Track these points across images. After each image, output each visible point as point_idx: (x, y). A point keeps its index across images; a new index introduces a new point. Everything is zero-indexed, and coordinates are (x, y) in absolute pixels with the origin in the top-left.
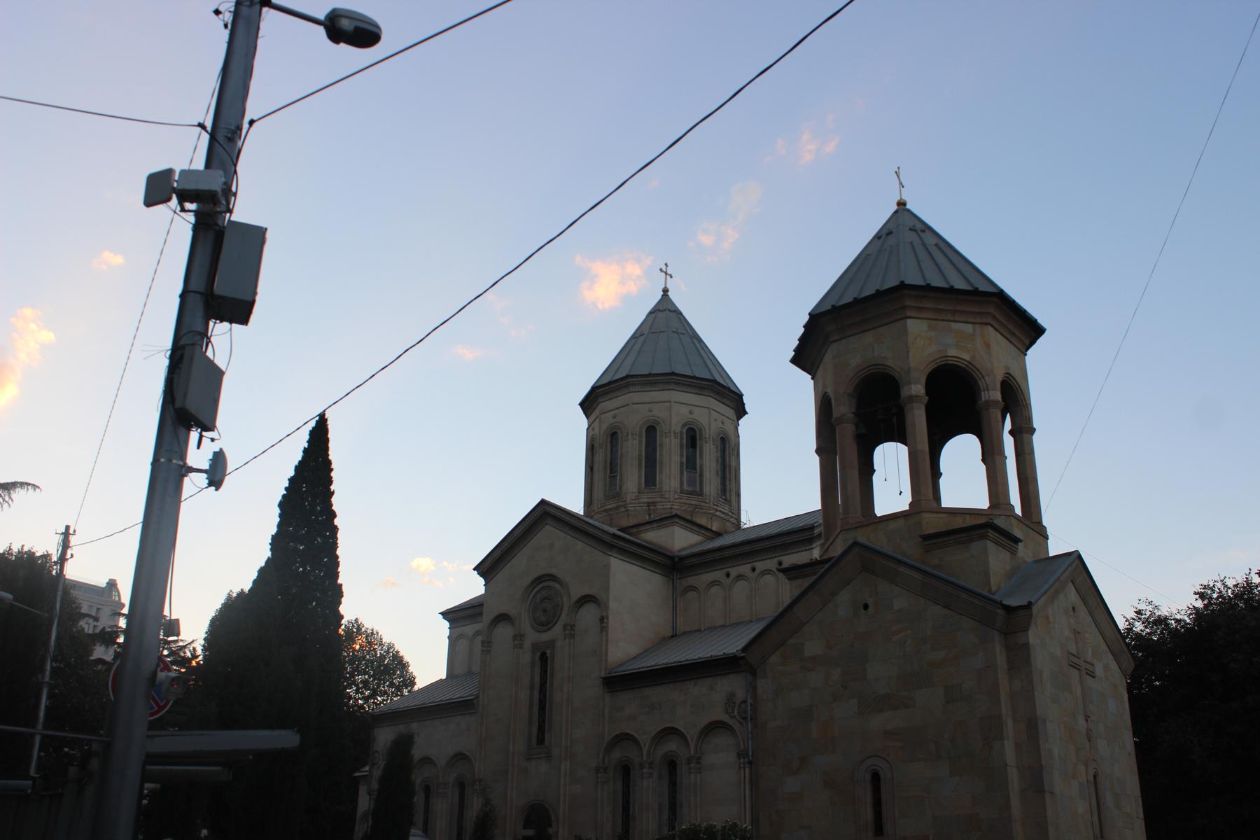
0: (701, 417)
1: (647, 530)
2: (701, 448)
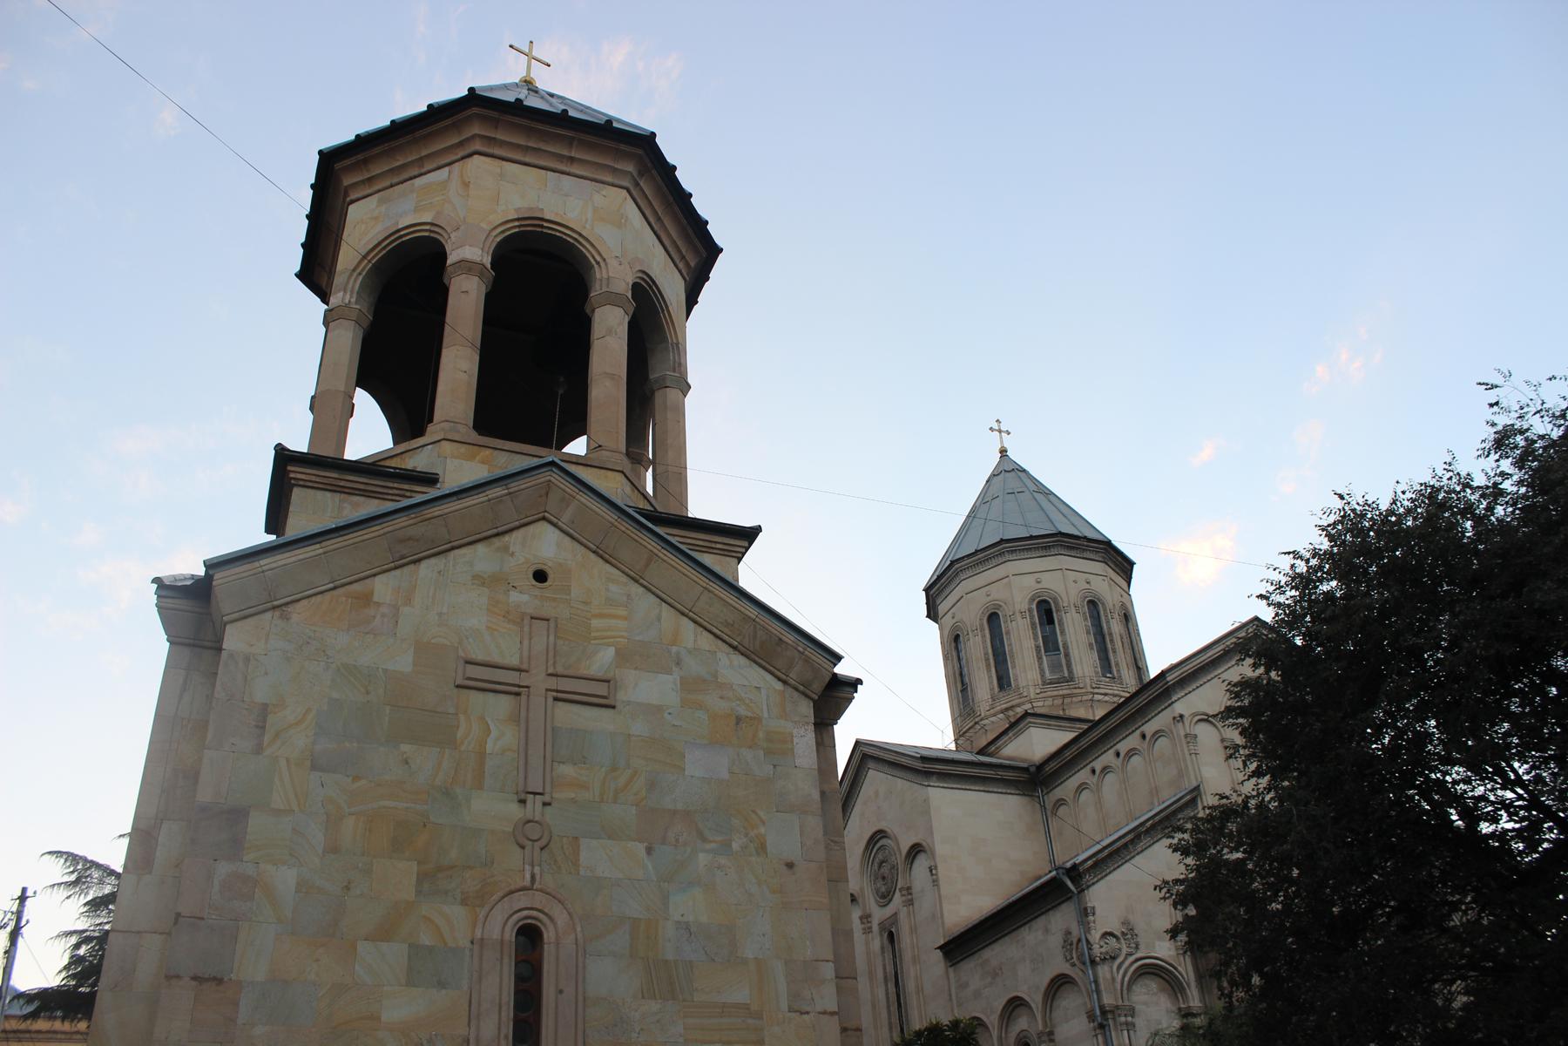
2: (1060, 622)
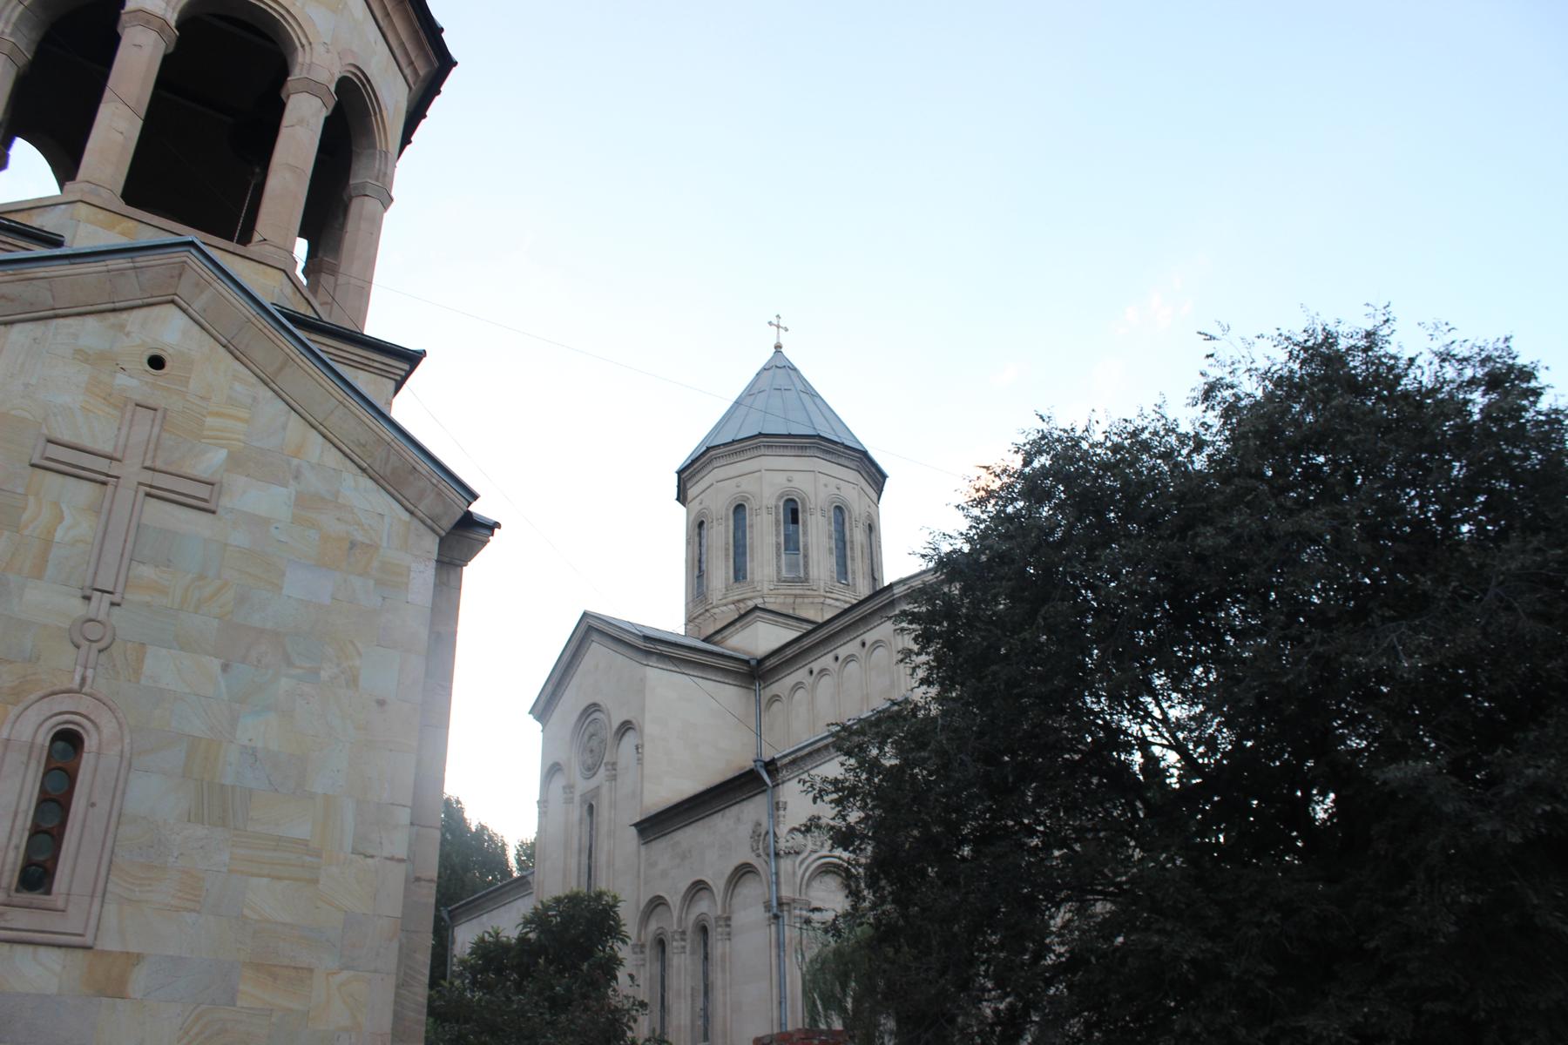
1: (732, 635)
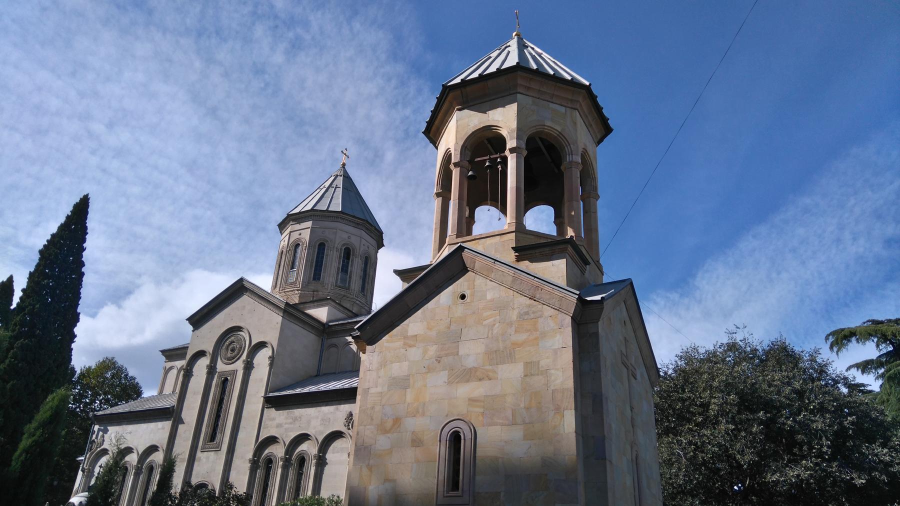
0: (355, 241)
1: (310, 308)
